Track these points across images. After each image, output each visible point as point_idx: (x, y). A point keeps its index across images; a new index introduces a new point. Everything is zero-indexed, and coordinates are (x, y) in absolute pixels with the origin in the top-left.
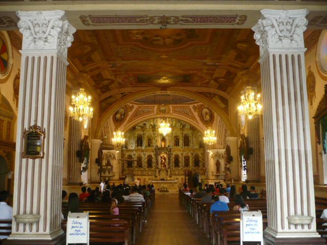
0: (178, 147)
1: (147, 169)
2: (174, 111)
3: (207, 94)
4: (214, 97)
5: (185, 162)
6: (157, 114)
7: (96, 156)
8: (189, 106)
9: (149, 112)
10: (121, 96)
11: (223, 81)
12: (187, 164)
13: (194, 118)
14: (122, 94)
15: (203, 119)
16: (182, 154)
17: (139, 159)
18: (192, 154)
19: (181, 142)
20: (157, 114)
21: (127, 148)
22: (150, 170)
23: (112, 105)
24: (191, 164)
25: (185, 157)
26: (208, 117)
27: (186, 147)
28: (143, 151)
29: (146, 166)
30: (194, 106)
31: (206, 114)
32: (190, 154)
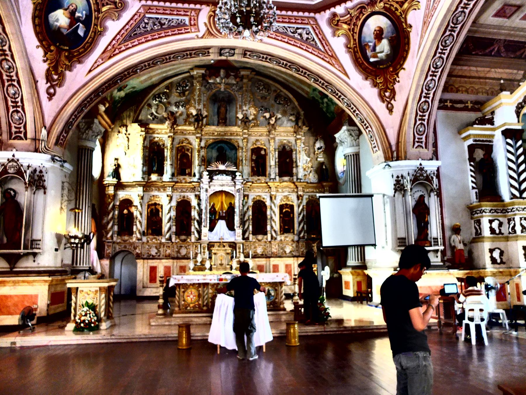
0: (263, 179)
6: (209, 33)
8: (315, 20)
9: (180, 27)
15: (367, 58)
19: (272, 161)
22: (184, 241)
25: (281, 207)
26: (384, 46)
27: (286, 178)
29: (174, 229)
30: (335, 15)
31: (379, 35)
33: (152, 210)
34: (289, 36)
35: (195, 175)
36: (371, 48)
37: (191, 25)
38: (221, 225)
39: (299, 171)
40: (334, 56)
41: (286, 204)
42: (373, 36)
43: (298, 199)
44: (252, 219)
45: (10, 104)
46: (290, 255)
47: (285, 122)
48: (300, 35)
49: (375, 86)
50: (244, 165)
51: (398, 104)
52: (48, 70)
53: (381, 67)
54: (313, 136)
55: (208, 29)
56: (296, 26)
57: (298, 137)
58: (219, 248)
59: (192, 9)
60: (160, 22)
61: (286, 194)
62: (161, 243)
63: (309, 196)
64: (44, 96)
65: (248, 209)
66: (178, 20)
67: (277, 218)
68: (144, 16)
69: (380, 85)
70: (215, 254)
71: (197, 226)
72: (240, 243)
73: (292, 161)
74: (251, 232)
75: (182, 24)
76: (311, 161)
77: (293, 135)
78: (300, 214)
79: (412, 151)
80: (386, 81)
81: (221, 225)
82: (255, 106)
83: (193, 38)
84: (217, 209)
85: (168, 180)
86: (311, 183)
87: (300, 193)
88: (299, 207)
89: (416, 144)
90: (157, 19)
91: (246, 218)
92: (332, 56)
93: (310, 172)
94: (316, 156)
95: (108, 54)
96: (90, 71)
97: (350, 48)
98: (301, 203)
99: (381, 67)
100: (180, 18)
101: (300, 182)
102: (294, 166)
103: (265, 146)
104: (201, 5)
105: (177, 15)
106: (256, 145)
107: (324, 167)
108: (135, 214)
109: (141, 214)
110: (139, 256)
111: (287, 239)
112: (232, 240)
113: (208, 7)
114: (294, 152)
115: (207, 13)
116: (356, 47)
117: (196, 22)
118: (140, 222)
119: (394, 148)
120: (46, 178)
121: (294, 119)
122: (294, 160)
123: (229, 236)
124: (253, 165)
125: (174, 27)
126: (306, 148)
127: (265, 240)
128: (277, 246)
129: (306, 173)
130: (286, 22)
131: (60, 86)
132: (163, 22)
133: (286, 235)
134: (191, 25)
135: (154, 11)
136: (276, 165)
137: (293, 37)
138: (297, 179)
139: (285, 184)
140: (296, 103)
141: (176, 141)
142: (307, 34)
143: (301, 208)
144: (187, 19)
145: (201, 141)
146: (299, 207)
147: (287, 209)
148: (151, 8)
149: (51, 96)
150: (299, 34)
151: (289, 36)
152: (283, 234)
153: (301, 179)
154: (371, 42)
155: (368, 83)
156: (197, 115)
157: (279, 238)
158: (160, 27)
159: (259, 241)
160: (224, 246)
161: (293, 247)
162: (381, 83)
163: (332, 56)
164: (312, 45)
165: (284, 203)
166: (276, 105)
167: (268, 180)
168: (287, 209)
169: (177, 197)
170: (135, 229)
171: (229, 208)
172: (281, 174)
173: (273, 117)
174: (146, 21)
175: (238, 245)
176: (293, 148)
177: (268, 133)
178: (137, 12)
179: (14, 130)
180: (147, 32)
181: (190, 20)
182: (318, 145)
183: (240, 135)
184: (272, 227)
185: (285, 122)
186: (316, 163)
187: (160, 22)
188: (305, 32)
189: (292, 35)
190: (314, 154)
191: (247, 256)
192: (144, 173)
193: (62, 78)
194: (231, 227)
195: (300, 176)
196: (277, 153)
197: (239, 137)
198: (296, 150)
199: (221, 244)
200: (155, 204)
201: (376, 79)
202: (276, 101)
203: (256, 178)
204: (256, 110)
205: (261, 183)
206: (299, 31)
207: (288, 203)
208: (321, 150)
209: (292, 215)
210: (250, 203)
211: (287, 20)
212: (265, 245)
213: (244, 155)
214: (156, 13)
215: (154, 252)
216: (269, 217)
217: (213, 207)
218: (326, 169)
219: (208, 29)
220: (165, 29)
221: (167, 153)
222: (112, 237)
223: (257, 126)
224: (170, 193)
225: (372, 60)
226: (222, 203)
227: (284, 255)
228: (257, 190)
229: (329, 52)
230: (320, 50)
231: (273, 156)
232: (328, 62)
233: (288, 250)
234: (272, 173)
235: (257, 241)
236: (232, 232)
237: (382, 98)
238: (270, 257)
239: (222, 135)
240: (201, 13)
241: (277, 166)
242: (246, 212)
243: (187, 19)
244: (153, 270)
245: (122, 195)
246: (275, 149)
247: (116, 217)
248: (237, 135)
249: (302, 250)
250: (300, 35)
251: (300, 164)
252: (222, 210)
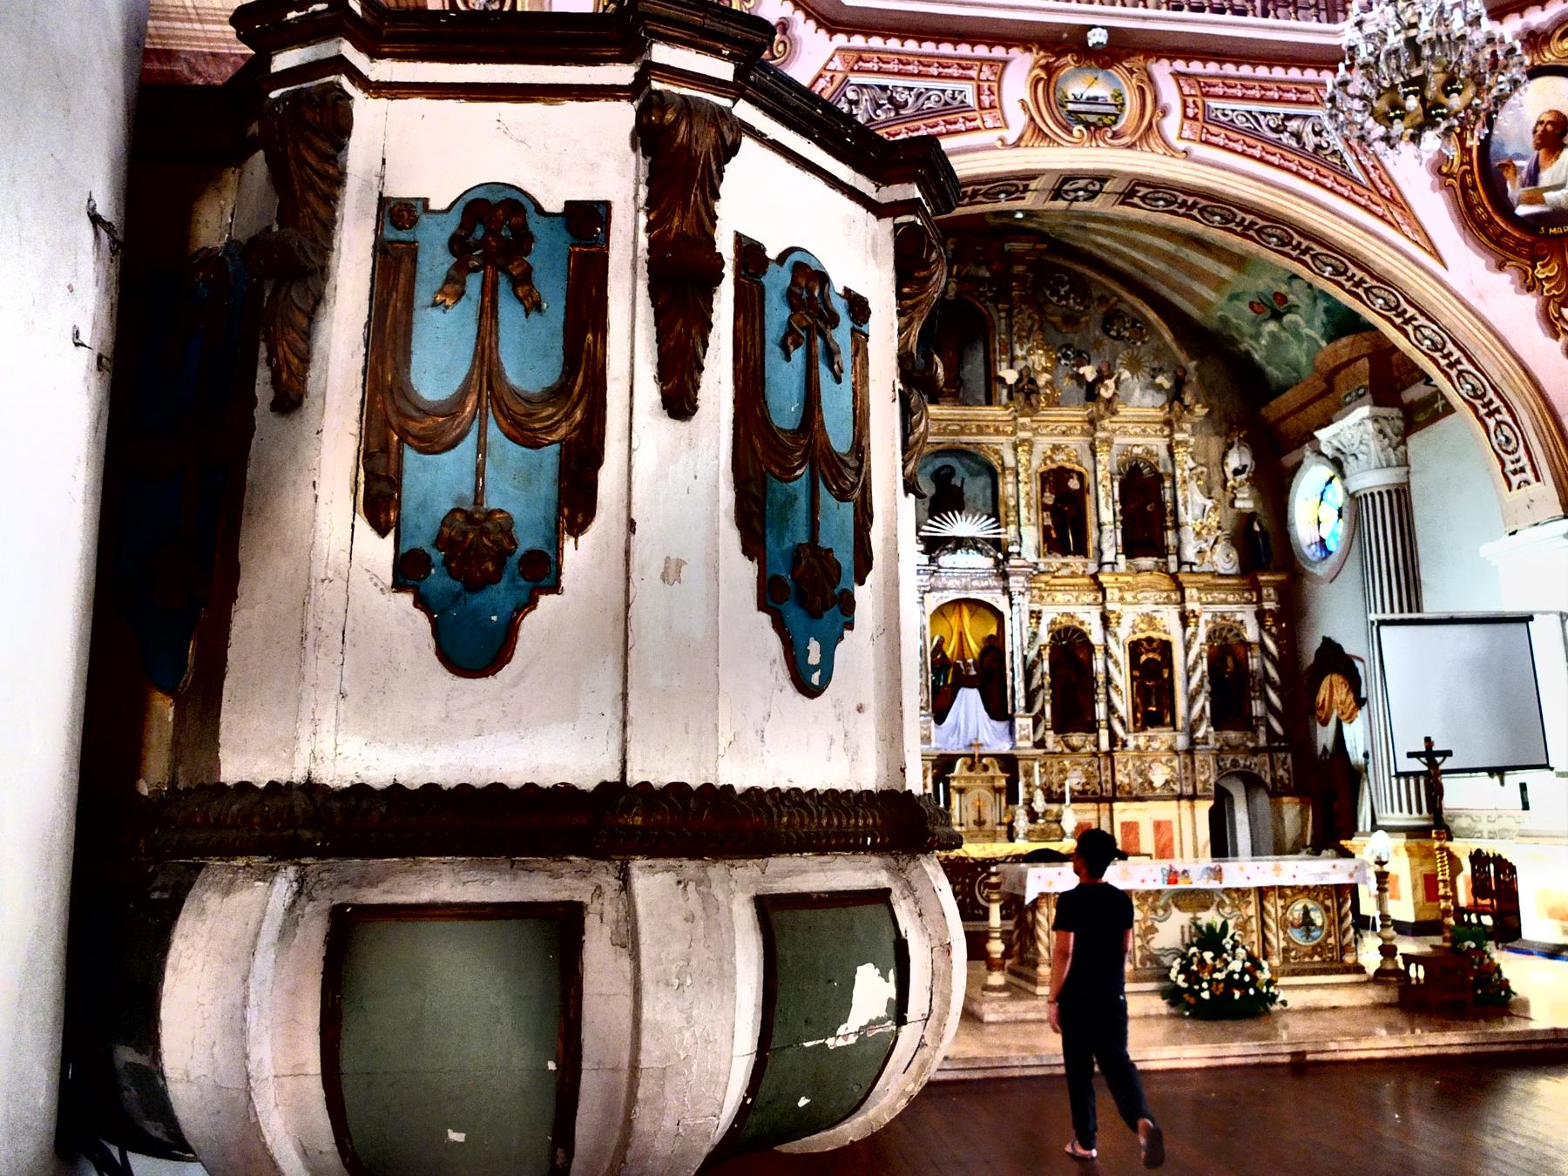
0: (1076, 562)
15: (1505, 207)
19: (1105, 510)
25: (1135, 648)
27: (1146, 562)
36: (1524, 174)
37: (982, 108)
38: (969, 702)
39: (1184, 538)
40: (1397, 201)
41: (1150, 640)
42: (1530, 140)
44: (1052, 685)
46: (1166, 793)
47: (1137, 393)
48: (1297, 136)
49: (1529, 289)
50: (1023, 521)
53: (1553, 231)
54: (1218, 434)
55: (1032, 119)
56: (1282, 109)
57: (1178, 436)
58: (972, 774)
59: (982, 60)
60: (891, 100)
61: (1148, 608)
63: (1215, 614)
65: (1039, 654)
66: (943, 91)
67: (1122, 679)
68: (845, 81)
69: (1547, 286)
70: (961, 791)
72: (1027, 758)
74: (1049, 725)
75: (956, 104)
76: (1215, 508)
77: (1162, 430)
81: (969, 702)
82: (1048, 346)
84: (949, 653)
88: (1187, 647)
90: (884, 88)
91: (1035, 682)
92: (1392, 200)
93: (1216, 542)
94: (1229, 495)
97: (1448, 175)
98: (1194, 635)
99: (1553, 231)
100: (950, 86)
101: (1192, 572)
103: (1080, 464)
104: (1008, 47)
105: (940, 76)
106: (1053, 461)
107: (1257, 528)
111: (1155, 745)
112: (1004, 747)
113: (1027, 54)
114: (1167, 484)
115: (1027, 71)
116: (1471, 172)
117: (995, 98)
121: (1167, 385)
122: (1169, 506)
123: (993, 738)
124: (1049, 522)
125: (932, 113)
126: (1200, 469)
127: (1090, 748)
128: (1130, 766)
129: (1204, 546)
130: (1253, 99)
132: (900, 98)
133: (1151, 732)
134: (982, 108)
135: (873, 66)
136: (1115, 522)
137: (1278, 144)
138: (1180, 563)
140: (1168, 336)
142: (1318, 134)
144: (969, 89)
146: (1187, 647)
147: (1151, 655)
148: (865, 56)
150: (1292, 134)
152: (1143, 729)
153: (1192, 564)
154: (1520, 157)
157: (1131, 743)
158: (893, 114)
159: (1074, 749)
160: (986, 768)
161: (1173, 768)
162: (1548, 279)
163: (1392, 200)
164: (1332, 167)
165: (1142, 636)
166: (1107, 341)
168: (1151, 655)
171: (984, 652)
173: (1110, 377)
174: (852, 96)
175: (1021, 764)
176: (1161, 470)
177: (1086, 426)
178: (825, 69)
181: (979, 93)
182: (1234, 461)
183: (1005, 433)
184: (1111, 709)
185: (1137, 393)
186: (1231, 512)
187: (891, 100)
188: (1309, 129)
189: (1274, 136)
190: (1224, 487)
191: (1053, 797)
194: (998, 708)
195: (1189, 554)
196: (1116, 484)
197: (1002, 439)
198: (1174, 477)
199: (974, 761)
201: (1534, 267)
202: (1106, 331)
203: (1056, 561)
204: (1049, 358)
205: (1073, 575)
206: (1293, 125)
207: (1155, 635)
208: (1244, 476)
210: (1045, 637)
211: (1256, 93)
212: (1090, 764)
213: (1022, 492)
214: (880, 71)
216: (1101, 679)
217: (938, 649)
218: (1263, 532)
219: (1032, 119)
220: (910, 118)
223: (1054, 403)
225: (1522, 210)
226: (961, 635)
227: (1149, 793)
228: (1059, 596)
229: (1382, 186)
230: (1356, 181)
231: (1107, 495)
232: (1382, 218)
233: (1159, 776)
234: (1105, 546)
235: (1067, 751)
236: (1001, 726)
238: (1112, 800)
239: (953, 433)
240: (1011, 71)
242: (1034, 664)
243: (969, 89)
246: (1112, 474)
248: (997, 432)
249: (1202, 778)
250: (1297, 136)
251: (1188, 517)
252: (963, 658)
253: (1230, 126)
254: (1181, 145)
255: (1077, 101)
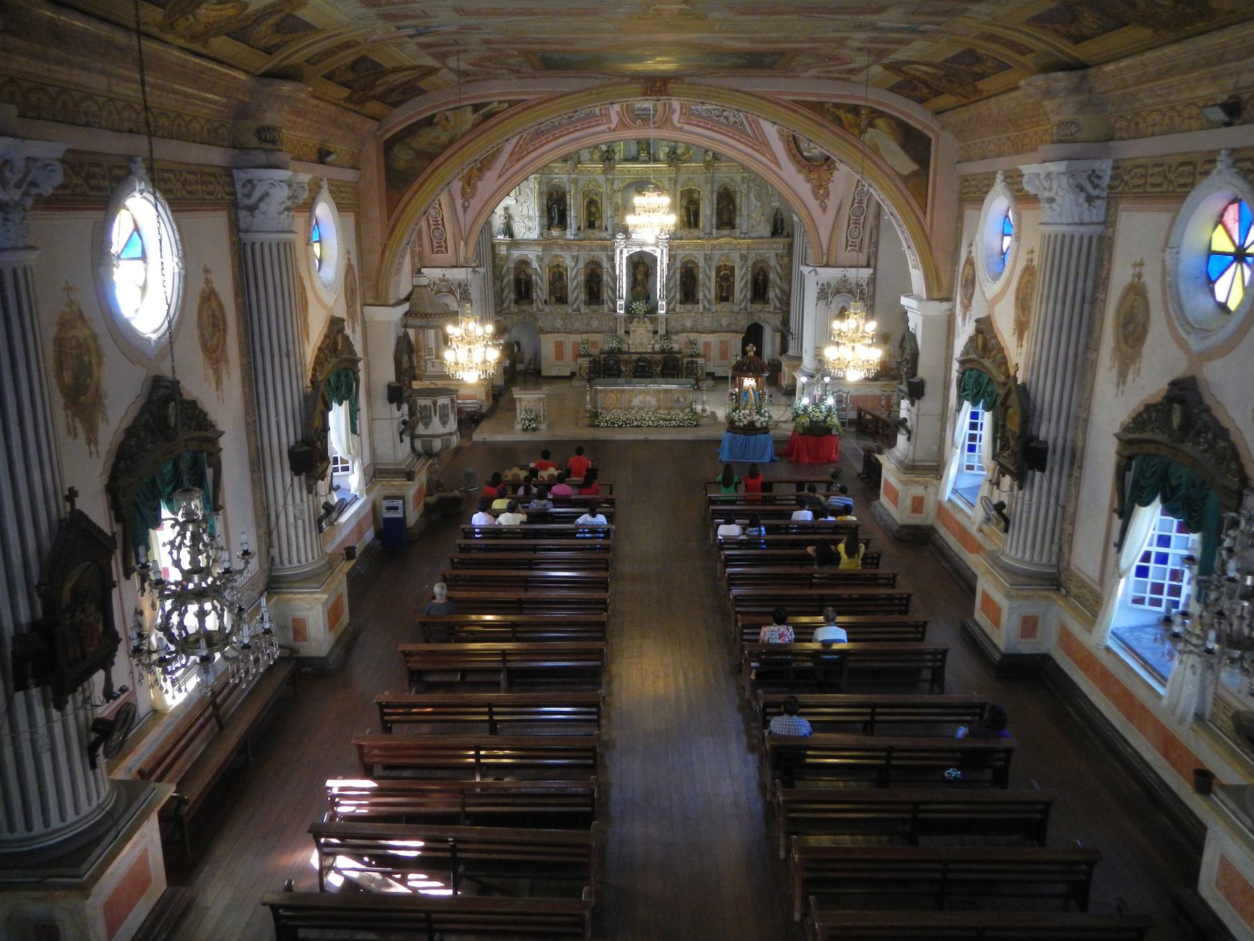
0: (695, 232)
1: (583, 309)
2: (689, 116)
3: (841, 113)
4: (871, 125)
5: (720, 287)
6: (622, 125)
7: (386, 373)
10: (470, 118)
11: (927, 74)
12: (725, 294)
13: (761, 144)
14: (476, 108)
16: (708, 258)
17: (558, 279)
18: (744, 258)
20: (622, 125)
21: (511, 236)
22: (594, 311)
23: (440, 159)
24: (738, 295)
25: (718, 269)
27: (725, 232)
28: (567, 246)
29: (582, 297)
32: (736, 256)
33: (554, 274)
34: (713, 121)
35: (606, 229)
41: (725, 266)
43: (741, 260)
45: (431, 222)
48: (726, 118)
51: (832, 203)
52: (463, 187)
62: (567, 314)
63: (756, 254)
64: (460, 210)
71: (611, 294)
73: (734, 207)
78: (742, 279)
79: (845, 255)
80: (820, 178)
83: (604, 132)
85: (572, 237)
86: (761, 238)
87: (744, 252)
89: (849, 248)
95: (515, 157)
96: (499, 176)
101: (744, 238)
102: (738, 214)
108: (534, 277)
109: (541, 279)
110: (542, 331)
118: (541, 290)
119: (825, 250)
120: (470, 291)
122: (738, 206)
131: (473, 196)
133: (723, 304)
137: (718, 122)
139: (722, 240)
141: (581, 183)
143: (744, 271)
145: (613, 184)
146: (741, 269)
149: (465, 209)
151: (713, 121)
155: (801, 177)
156: (608, 151)
159: (689, 311)
167: (702, 235)
169: (584, 257)
170: (534, 297)
172: (720, 226)
179: (435, 244)
180: (555, 128)
184: (705, 296)
192: (542, 227)
193: (474, 188)
196: (715, 196)
200: (558, 266)
206: (725, 113)
209: (731, 279)
210: (679, 265)
215: (559, 323)
216: (701, 282)
220: (574, 122)
221: (570, 201)
222: (509, 307)
224: (575, 254)
225: (805, 154)
233: (724, 322)
237: (816, 195)
241: (715, 215)
244: (559, 345)
245: (516, 254)
246: (712, 192)
247: (512, 282)
253: (700, 116)
254: (679, 125)
255: (639, 110)
